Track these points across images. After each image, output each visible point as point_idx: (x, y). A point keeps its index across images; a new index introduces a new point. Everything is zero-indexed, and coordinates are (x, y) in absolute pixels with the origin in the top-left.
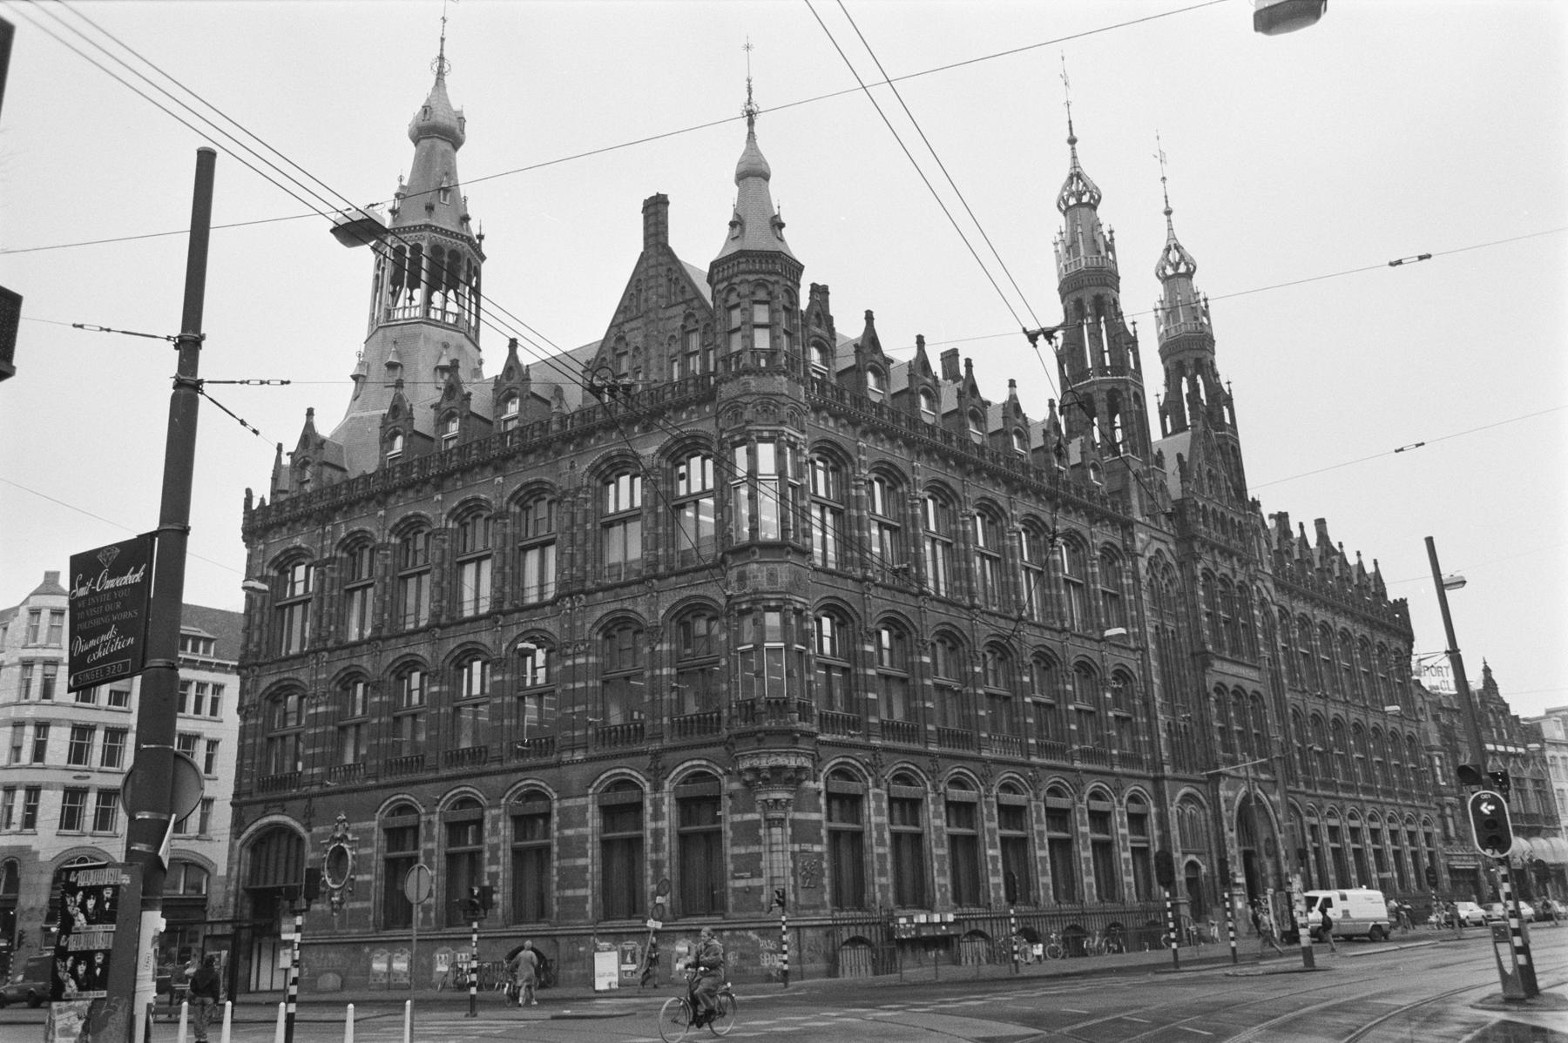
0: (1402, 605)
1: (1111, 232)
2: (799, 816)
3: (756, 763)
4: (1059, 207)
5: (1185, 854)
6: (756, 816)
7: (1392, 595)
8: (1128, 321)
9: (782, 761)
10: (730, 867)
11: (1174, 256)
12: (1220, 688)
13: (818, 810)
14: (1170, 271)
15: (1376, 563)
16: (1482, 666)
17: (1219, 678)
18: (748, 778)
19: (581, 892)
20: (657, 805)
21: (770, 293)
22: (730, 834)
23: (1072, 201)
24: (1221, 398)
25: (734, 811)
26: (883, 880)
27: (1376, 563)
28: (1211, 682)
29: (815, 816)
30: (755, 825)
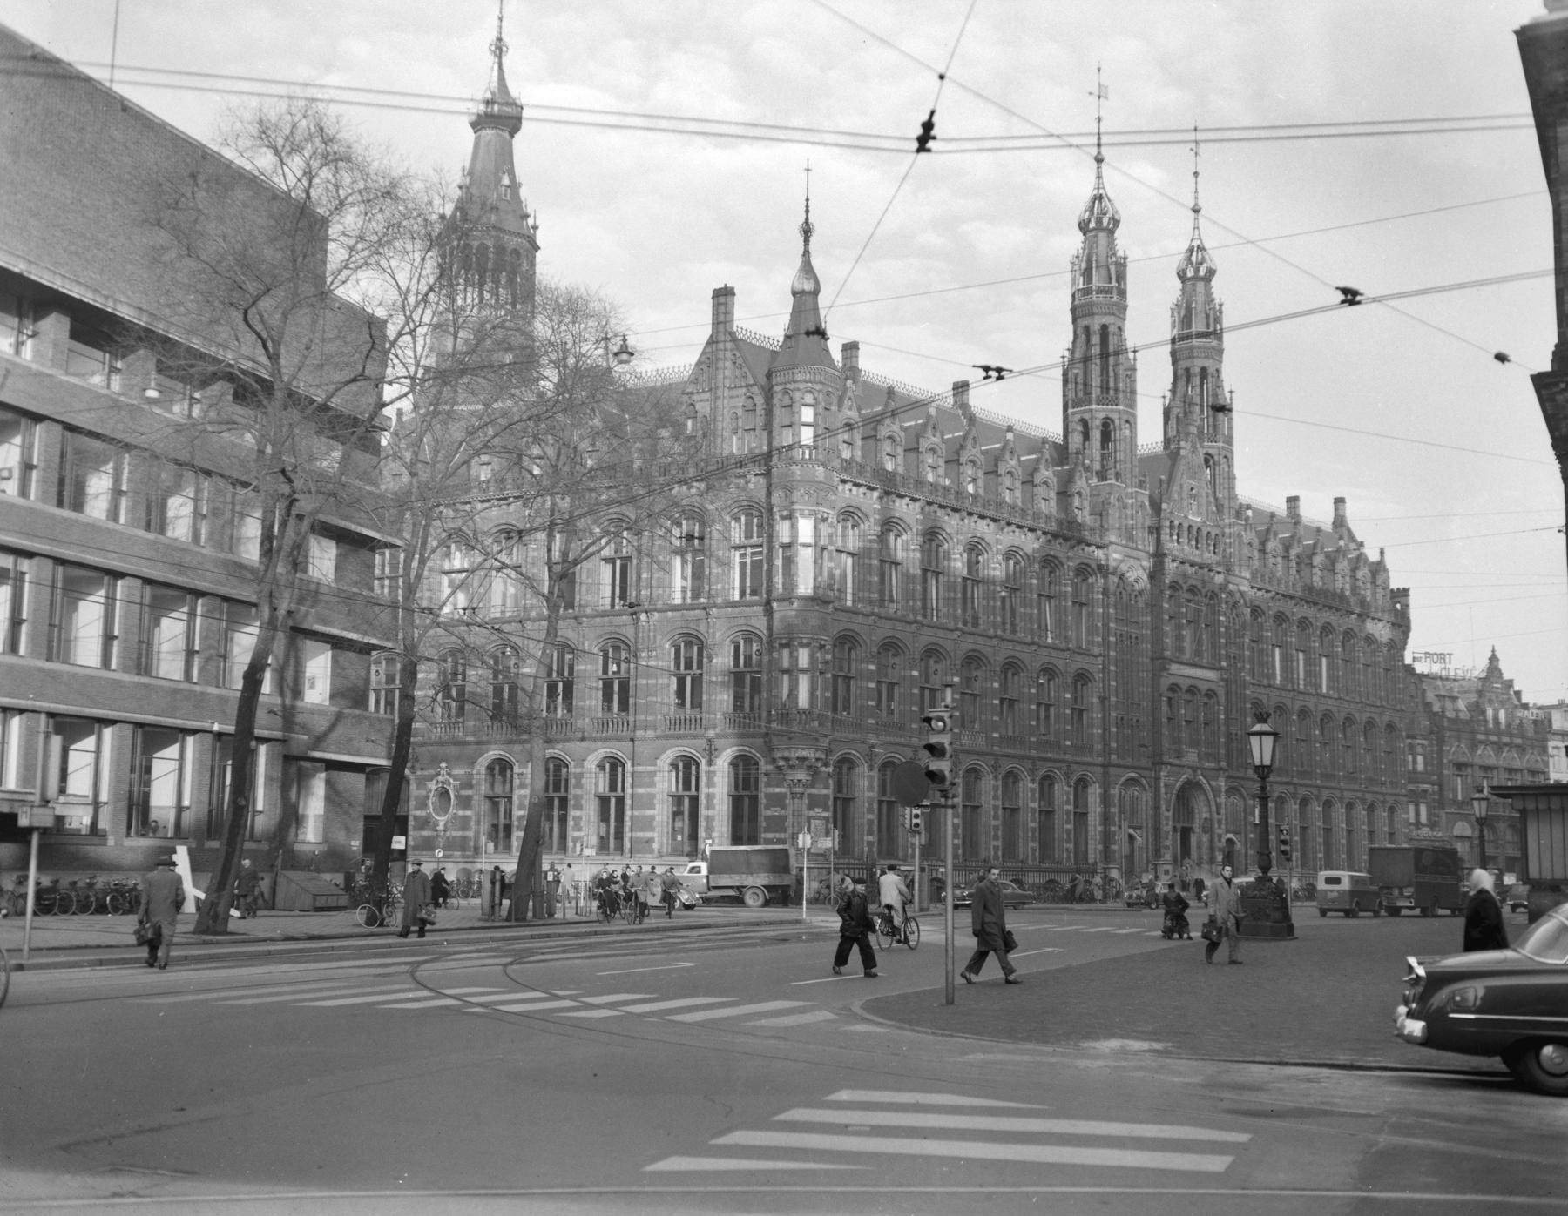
0: (1404, 593)
2: (813, 791)
3: (786, 754)
6: (783, 790)
9: (805, 753)
10: (764, 824)
12: (1174, 688)
13: (827, 787)
15: (1382, 552)
16: (1489, 654)
17: (1172, 680)
18: (781, 763)
19: (649, 835)
20: (710, 775)
21: (815, 399)
22: (764, 801)
25: (768, 785)
26: (871, 838)
27: (1382, 552)
28: (1165, 682)
30: (783, 796)
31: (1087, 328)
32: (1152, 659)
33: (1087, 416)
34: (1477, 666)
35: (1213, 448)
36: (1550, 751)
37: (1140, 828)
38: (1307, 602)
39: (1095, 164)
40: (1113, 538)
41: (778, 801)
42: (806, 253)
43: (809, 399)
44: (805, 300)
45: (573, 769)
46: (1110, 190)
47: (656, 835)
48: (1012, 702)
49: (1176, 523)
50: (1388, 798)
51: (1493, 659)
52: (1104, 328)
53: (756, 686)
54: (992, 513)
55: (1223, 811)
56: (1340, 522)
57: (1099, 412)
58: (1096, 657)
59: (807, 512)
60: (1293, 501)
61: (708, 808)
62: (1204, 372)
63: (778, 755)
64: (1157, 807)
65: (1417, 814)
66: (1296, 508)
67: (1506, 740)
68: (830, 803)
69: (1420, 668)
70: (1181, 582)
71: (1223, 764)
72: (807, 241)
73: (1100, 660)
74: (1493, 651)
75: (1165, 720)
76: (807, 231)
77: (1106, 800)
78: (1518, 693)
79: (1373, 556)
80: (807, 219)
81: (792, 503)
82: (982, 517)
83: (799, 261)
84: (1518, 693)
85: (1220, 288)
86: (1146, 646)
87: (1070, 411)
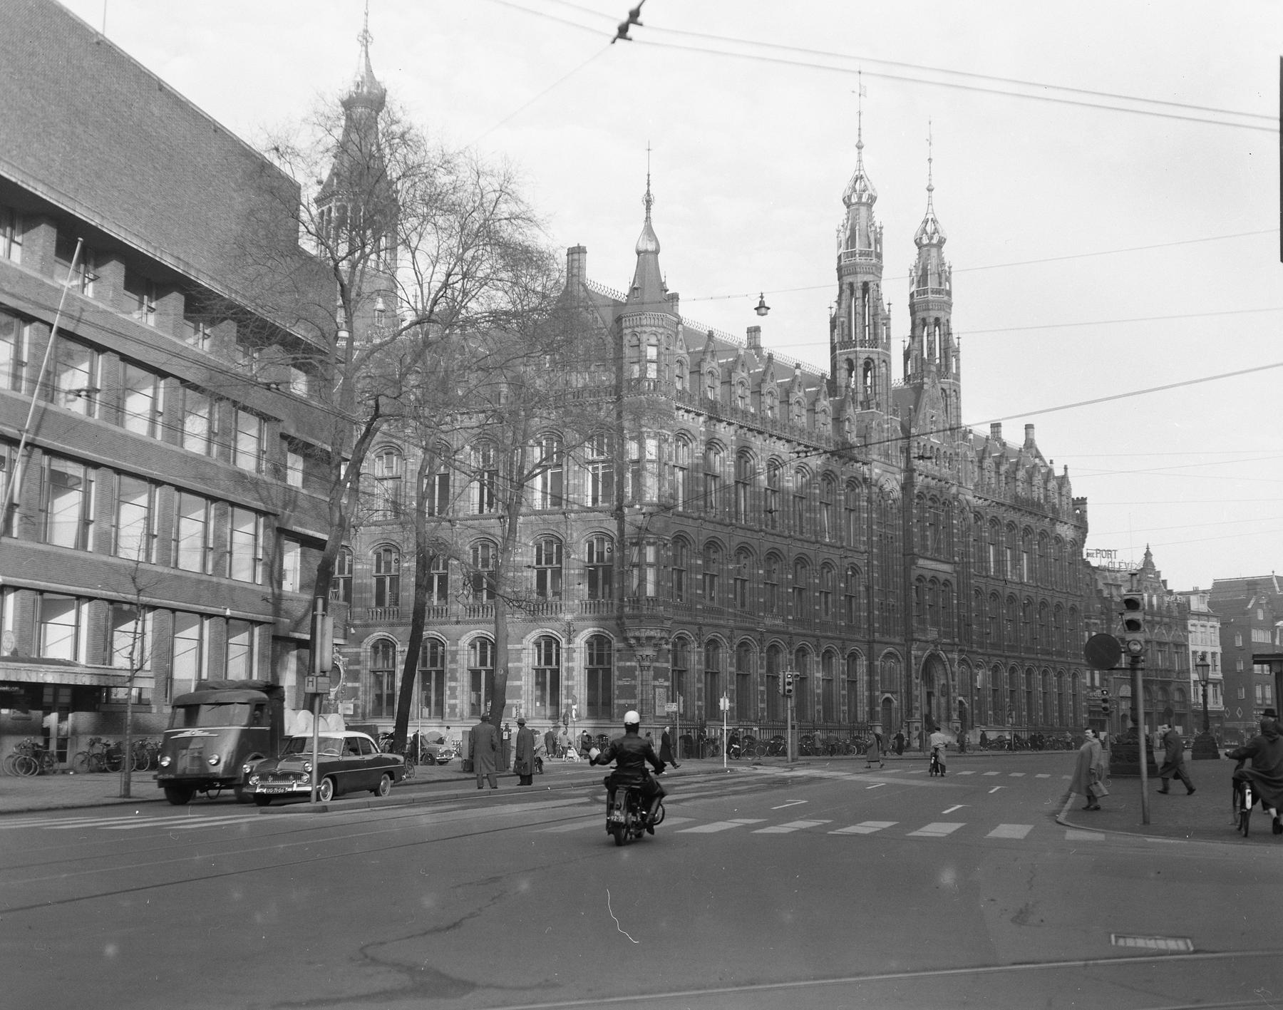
0: (1082, 501)
1: (881, 228)
2: (657, 664)
3: (637, 634)
4: (843, 200)
5: (883, 692)
6: (634, 664)
7: (1075, 494)
8: (885, 301)
9: (652, 633)
10: (617, 692)
11: (930, 228)
12: (920, 579)
13: (668, 662)
14: (925, 241)
15: (1066, 468)
17: (919, 572)
21: (658, 340)
22: (616, 673)
23: (854, 200)
24: (949, 351)
25: (620, 659)
26: (700, 703)
27: (1066, 468)
28: (915, 573)
29: (665, 665)
30: (633, 669)
31: (851, 285)
32: (904, 555)
33: (852, 357)
34: (1134, 560)
35: (946, 383)
36: (1190, 628)
37: (896, 693)
38: (1014, 509)
39: (856, 150)
40: (875, 457)
41: (629, 673)
42: (648, 218)
43: (653, 340)
44: (647, 260)
45: (448, 647)
46: (868, 172)
47: (523, 702)
48: (800, 590)
49: (922, 444)
50: (1043, 664)
51: (1148, 555)
52: (866, 284)
53: (608, 579)
54: (787, 435)
55: (956, 679)
56: (1029, 444)
57: (862, 353)
58: (862, 553)
59: (652, 435)
60: (996, 427)
61: (568, 679)
62: (937, 322)
63: (630, 634)
64: (909, 676)
65: (1093, 679)
66: (999, 432)
67: (1157, 619)
68: (670, 674)
69: (1094, 562)
70: (925, 492)
71: (956, 640)
72: (648, 209)
73: (865, 556)
74: (1148, 548)
75: (914, 604)
76: (649, 203)
77: (871, 670)
78: (1164, 582)
79: (1058, 472)
80: (648, 190)
81: (641, 426)
82: (779, 439)
83: (642, 226)
84: (1164, 582)
85: (950, 254)
86: (899, 544)
87: (838, 352)
